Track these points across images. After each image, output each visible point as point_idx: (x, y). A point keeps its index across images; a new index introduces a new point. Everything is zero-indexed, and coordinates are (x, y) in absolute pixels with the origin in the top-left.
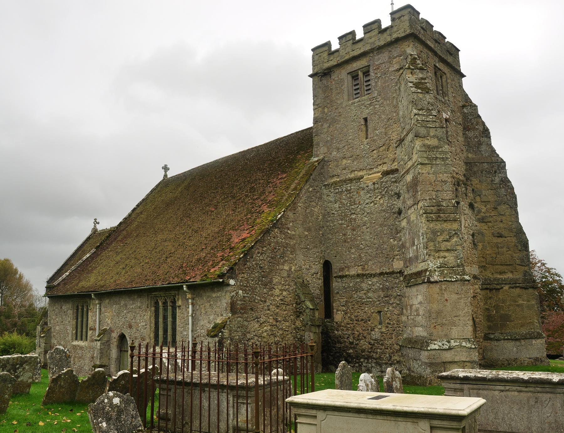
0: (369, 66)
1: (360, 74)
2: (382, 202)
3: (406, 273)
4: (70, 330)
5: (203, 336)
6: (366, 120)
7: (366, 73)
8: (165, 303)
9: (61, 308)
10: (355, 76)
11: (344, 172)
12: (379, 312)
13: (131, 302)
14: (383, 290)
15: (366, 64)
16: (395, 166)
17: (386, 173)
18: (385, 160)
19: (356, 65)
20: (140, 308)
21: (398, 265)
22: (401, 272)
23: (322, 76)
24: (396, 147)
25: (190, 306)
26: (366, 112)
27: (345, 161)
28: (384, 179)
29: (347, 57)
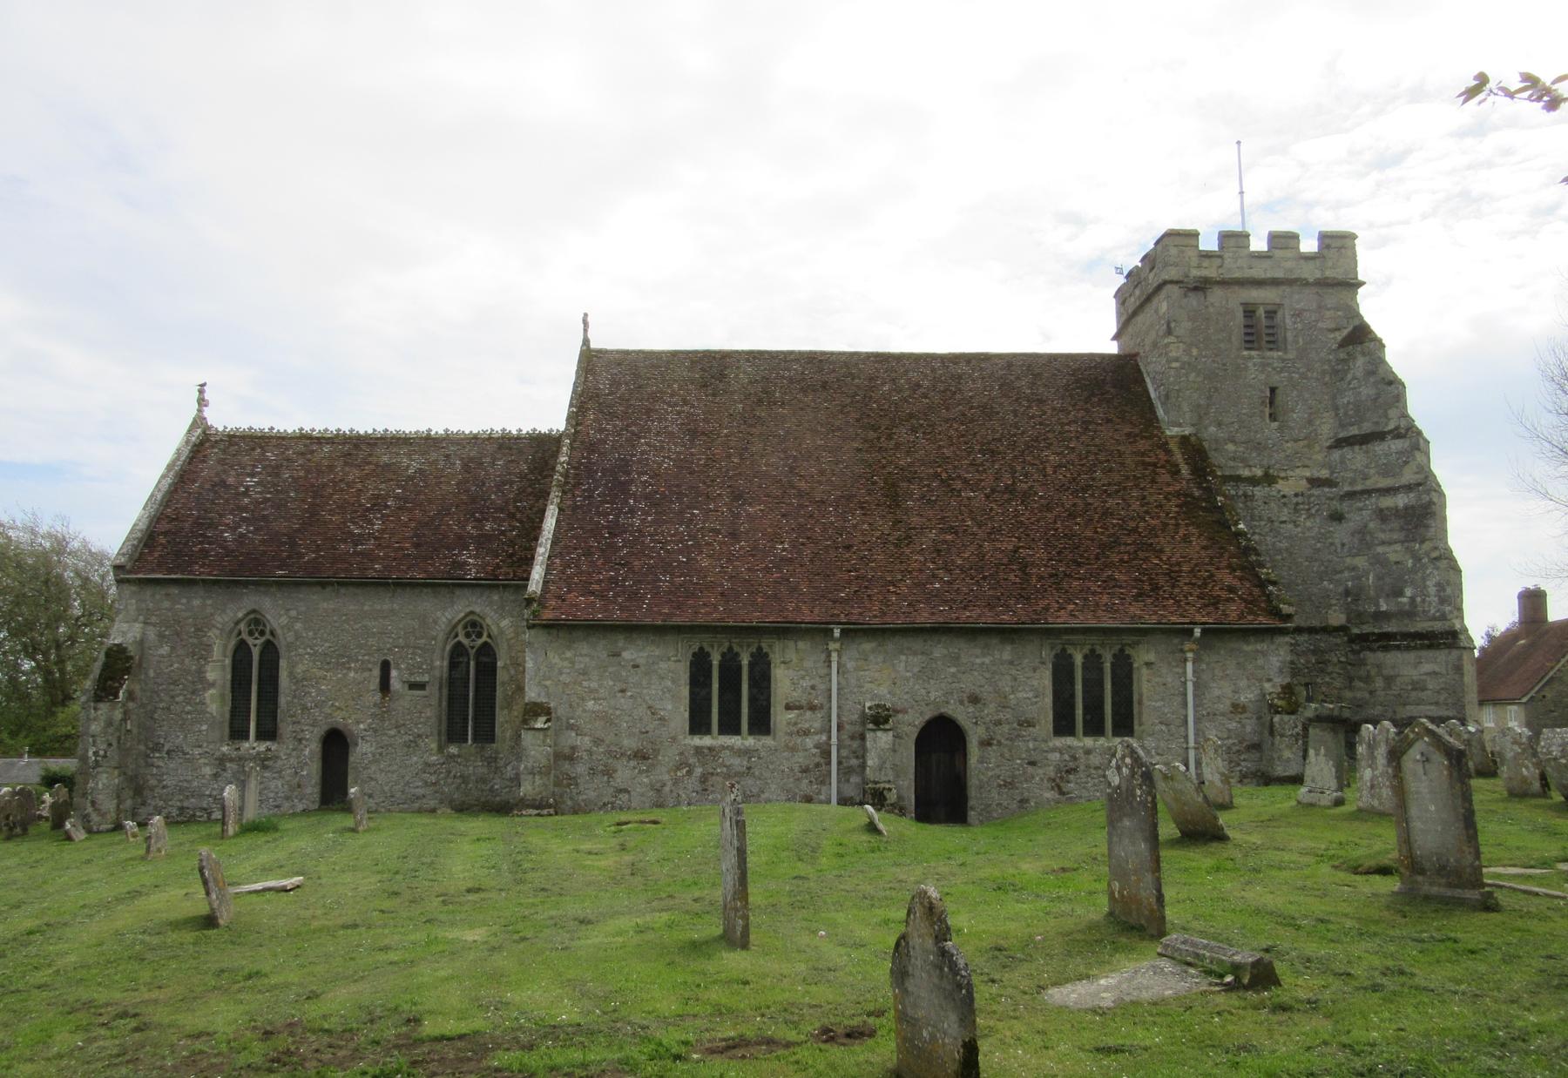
0: (1280, 305)
1: (1261, 312)
2: (1308, 524)
3: (1356, 631)
4: (679, 714)
5: (1223, 714)
6: (1273, 390)
7: (1271, 314)
8: (1093, 660)
9: (617, 655)
10: (1249, 312)
11: (1232, 463)
12: (1307, 685)
13: (978, 651)
14: (1314, 652)
15: (1278, 301)
16: (1324, 474)
17: (1314, 482)
18: (1307, 462)
19: (1255, 295)
20: (1011, 663)
21: (1337, 618)
22: (1342, 629)
23: (1190, 290)
24: (1330, 447)
25: (1189, 666)
26: (1275, 379)
27: (1231, 447)
28: (1316, 492)
29: (1237, 275)
